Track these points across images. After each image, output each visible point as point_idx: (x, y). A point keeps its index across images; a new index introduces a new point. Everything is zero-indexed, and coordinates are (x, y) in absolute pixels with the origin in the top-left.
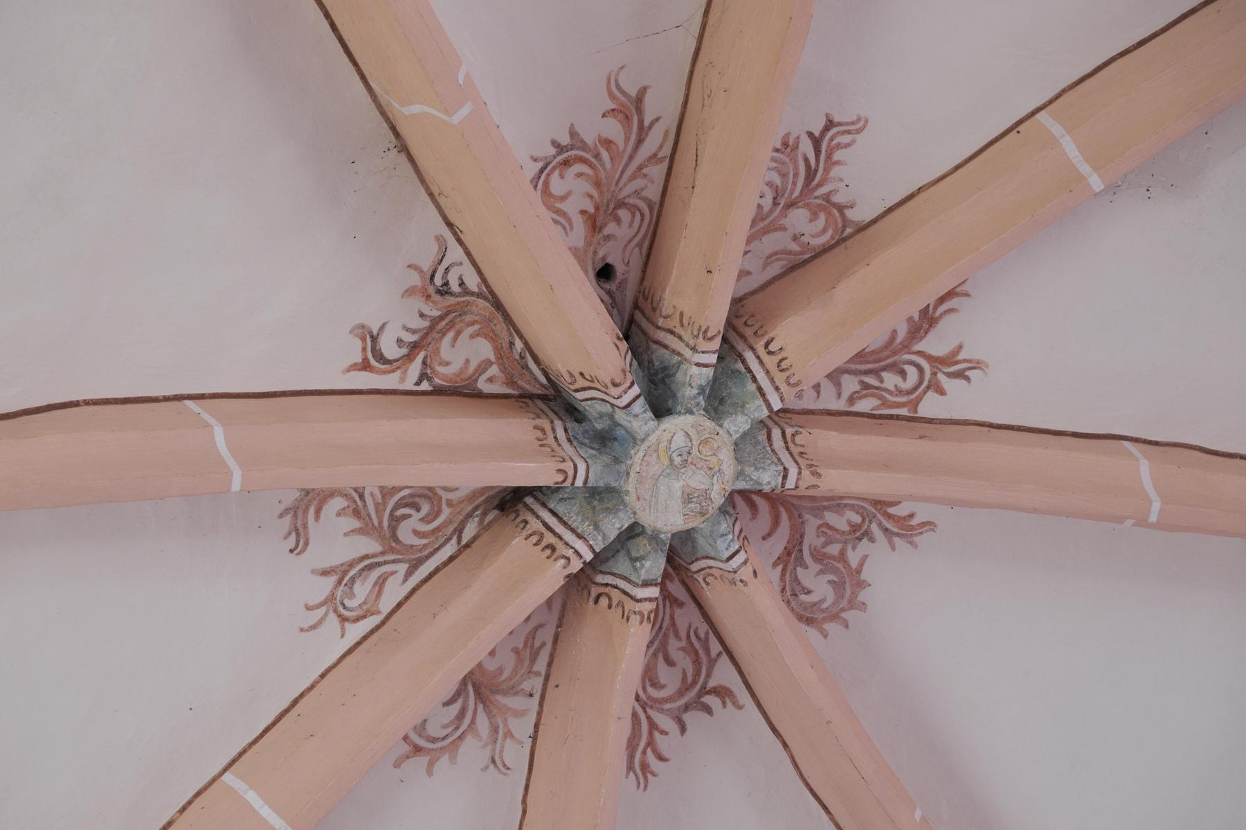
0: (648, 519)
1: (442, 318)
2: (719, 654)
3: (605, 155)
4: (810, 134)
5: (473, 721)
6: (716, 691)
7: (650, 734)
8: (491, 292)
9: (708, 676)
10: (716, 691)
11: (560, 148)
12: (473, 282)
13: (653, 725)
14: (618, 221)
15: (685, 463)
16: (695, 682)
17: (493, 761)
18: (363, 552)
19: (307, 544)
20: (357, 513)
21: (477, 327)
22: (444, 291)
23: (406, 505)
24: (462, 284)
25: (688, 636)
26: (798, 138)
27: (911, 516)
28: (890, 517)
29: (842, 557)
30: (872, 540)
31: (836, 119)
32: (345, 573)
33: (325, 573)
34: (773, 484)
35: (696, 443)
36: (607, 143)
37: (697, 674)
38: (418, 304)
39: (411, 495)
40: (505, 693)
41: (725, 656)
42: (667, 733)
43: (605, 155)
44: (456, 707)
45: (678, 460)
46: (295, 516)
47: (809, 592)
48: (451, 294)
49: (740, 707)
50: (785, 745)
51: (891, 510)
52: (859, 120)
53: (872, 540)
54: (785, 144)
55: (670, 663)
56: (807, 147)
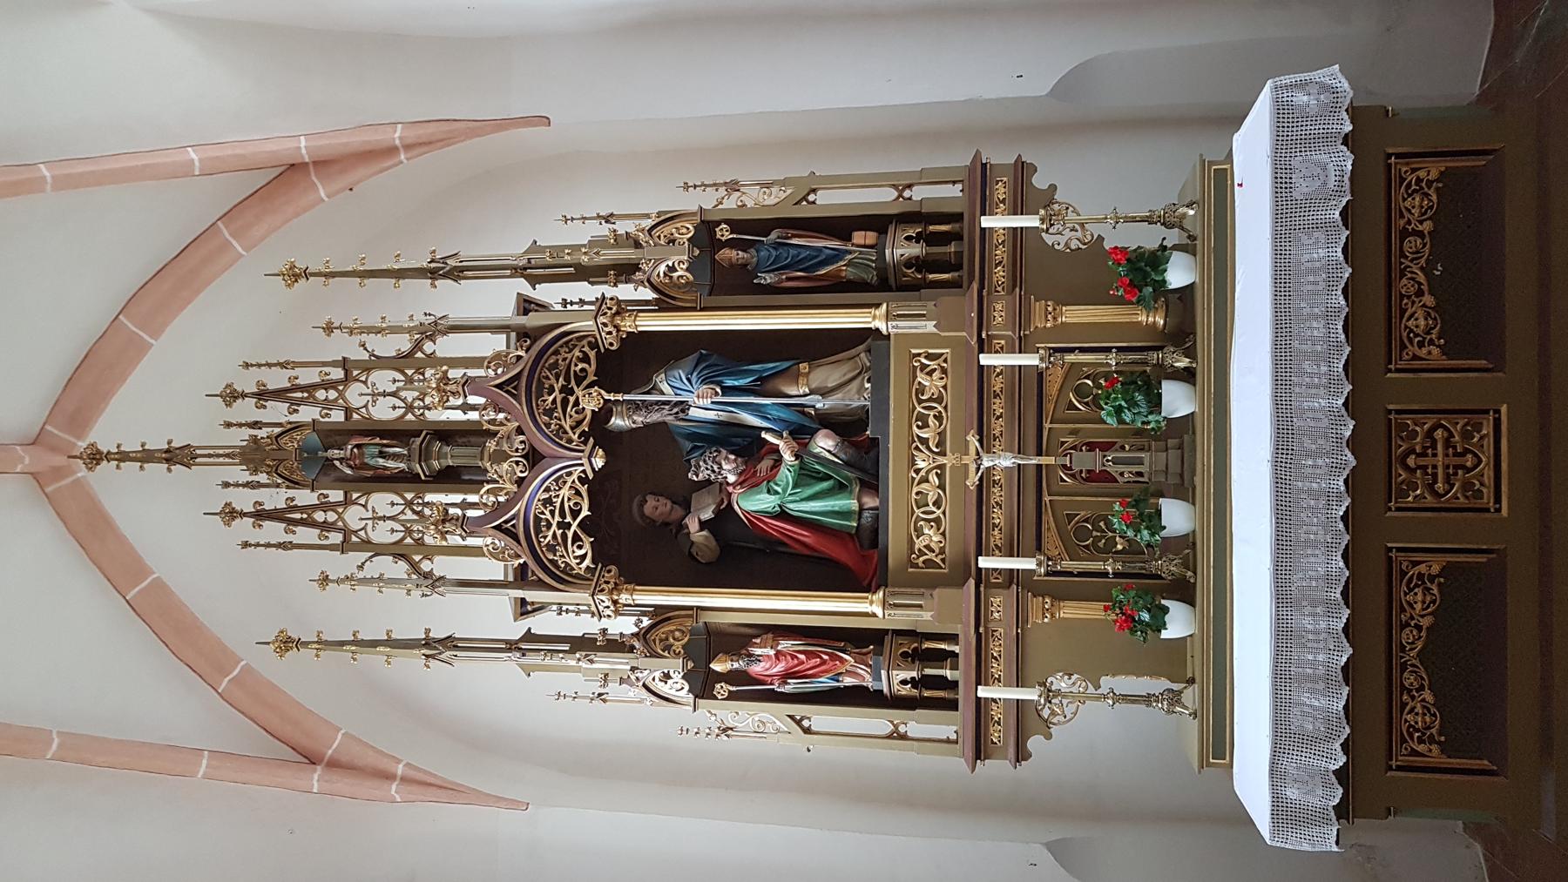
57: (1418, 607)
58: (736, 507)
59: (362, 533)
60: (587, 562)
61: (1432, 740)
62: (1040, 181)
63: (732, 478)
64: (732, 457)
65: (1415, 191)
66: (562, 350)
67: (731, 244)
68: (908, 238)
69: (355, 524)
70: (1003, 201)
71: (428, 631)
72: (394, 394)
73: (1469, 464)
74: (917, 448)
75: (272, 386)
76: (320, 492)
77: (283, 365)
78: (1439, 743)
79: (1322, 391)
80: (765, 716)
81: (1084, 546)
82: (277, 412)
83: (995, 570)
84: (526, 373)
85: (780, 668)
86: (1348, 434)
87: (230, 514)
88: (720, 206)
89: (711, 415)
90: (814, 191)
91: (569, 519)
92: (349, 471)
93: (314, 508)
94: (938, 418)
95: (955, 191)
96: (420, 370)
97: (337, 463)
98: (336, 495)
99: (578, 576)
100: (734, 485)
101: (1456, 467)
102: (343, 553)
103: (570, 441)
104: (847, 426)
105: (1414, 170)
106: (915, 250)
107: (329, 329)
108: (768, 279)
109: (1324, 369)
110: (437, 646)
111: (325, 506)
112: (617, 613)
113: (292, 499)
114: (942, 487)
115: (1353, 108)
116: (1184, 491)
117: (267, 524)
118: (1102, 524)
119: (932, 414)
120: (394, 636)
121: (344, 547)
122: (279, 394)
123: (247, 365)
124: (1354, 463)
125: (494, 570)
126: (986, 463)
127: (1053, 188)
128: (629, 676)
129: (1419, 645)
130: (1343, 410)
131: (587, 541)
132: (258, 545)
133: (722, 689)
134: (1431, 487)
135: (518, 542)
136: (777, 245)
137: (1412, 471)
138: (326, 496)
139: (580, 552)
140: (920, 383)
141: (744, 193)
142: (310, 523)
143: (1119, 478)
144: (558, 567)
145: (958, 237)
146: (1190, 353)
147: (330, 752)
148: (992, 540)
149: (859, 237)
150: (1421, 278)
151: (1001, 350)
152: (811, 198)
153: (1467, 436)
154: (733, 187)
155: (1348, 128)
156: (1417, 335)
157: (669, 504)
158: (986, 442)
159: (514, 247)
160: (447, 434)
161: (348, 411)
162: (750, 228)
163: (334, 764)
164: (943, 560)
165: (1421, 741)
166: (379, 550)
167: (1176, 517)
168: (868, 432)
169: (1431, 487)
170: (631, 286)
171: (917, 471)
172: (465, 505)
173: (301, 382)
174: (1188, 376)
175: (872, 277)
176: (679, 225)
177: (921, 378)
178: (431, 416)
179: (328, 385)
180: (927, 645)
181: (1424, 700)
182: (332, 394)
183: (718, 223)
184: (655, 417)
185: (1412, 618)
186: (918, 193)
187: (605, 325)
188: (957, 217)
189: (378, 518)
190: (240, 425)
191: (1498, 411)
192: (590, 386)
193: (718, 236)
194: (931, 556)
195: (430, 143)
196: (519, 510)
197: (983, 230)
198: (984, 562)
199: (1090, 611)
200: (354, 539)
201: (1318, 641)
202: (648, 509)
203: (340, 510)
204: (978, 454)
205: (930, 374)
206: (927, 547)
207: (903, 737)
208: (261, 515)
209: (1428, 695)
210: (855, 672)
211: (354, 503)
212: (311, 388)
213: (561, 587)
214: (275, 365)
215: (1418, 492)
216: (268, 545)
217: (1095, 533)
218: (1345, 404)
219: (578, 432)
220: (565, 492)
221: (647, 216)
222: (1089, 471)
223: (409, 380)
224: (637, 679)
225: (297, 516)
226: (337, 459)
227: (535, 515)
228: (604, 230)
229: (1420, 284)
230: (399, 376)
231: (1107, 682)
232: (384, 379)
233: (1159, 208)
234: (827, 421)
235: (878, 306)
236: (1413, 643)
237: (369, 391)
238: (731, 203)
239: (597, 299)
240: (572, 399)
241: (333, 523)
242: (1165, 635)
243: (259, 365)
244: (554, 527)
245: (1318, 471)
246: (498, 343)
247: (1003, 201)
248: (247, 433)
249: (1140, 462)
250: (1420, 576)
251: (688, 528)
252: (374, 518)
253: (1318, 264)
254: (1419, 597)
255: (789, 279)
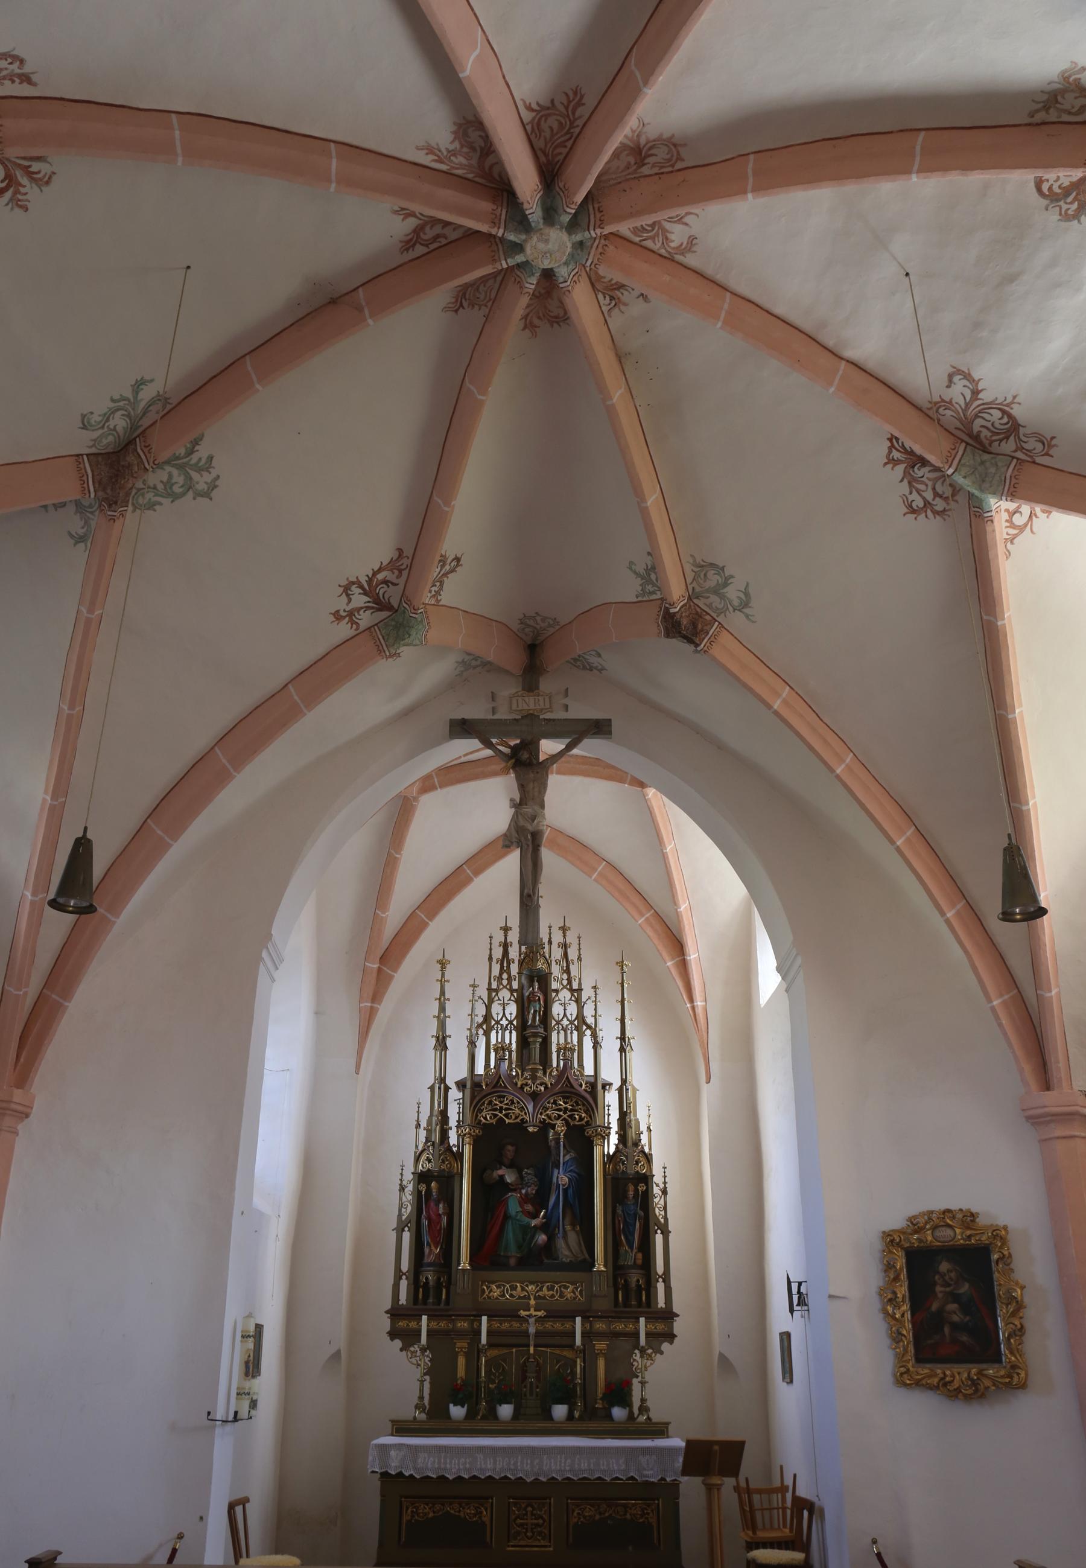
0: (564, 236)
1: (615, 289)
2: (527, 124)
3: (541, 315)
4: (464, 308)
5: (647, 143)
6: (532, 110)
7: (568, 105)
8: (594, 290)
9: (534, 119)
10: (532, 110)
11: (557, 323)
12: (600, 296)
13: (567, 108)
14: (539, 292)
15: (545, 253)
16: (542, 116)
17: (643, 124)
18: (669, 223)
19: (690, 237)
20: (667, 239)
21: (602, 280)
22: (612, 298)
23: (646, 230)
24: (605, 297)
25: (540, 136)
26: (468, 307)
27: (427, 154)
28: (438, 156)
29: (462, 146)
30: (447, 149)
31: (454, 313)
32: (679, 220)
33: (686, 224)
34: (509, 234)
35: (540, 259)
36: (539, 318)
37: (540, 119)
38: (623, 298)
39: (642, 232)
40: (629, 146)
41: (525, 121)
42: (561, 103)
43: (541, 315)
44: (651, 152)
45: (548, 255)
46: (690, 249)
47: (480, 136)
48: (609, 295)
49: (522, 100)
50: (504, 77)
51: (436, 158)
52: (445, 311)
53: (447, 149)
54: (473, 306)
55: (551, 128)
56: (465, 304)
57: (468, 1511)
58: (510, 1194)
59: (496, 998)
60: (483, 1121)
61: (413, 1516)
62: (665, 1346)
63: (523, 1191)
64: (534, 1192)
65: (643, 1511)
66: (585, 1108)
67: (636, 1190)
68: (638, 1281)
69: (501, 994)
70: (656, 1328)
71: (450, 1037)
72: (565, 1015)
73: (528, 1534)
74: (537, 1286)
75: (569, 950)
76: (517, 976)
77: (580, 959)
78: (412, 1519)
79: (558, 1468)
80: (409, 1209)
81: (491, 1370)
82: (557, 953)
83: (481, 1324)
84: (574, 1091)
85: (434, 1217)
86: (540, 1478)
87: (506, 929)
88: (654, 1185)
89: (555, 1180)
90: (662, 1233)
91: (504, 1112)
92: (527, 994)
93: (509, 974)
94: (552, 1296)
95: (661, 1303)
96: (577, 1028)
97: (531, 989)
98: (515, 985)
99: (477, 1116)
100: (521, 1193)
101: (527, 1529)
102: (487, 989)
103: (541, 1114)
104: (549, 1248)
105: (652, 1511)
106: (633, 1285)
107: (595, 988)
108: (619, 1211)
109: (567, 1468)
110: (441, 1043)
111: (509, 979)
112: (459, 1136)
113: (513, 962)
114: (520, 1298)
115: (678, 1484)
116: (516, 1416)
117: (501, 949)
118: (501, 1377)
119: (555, 1293)
120: (447, 1019)
121: (490, 990)
122: (566, 955)
123: (579, 938)
124: (528, 1481)
125: (480, 1070)
126: (531, 1320)
127: (662, 1353)
128: (430, 1141)
129: (452, 1512)
130: (550, 1477)
131: (494, 1121)
132: (491, 944)
133: (423, 1188)
134: (518, 1517)
135: (494, 1087)
136: (635, 1214)
137: (525, 1509)
138: (515, 980)
139: (488, 1118)
140: (569, 1287)
141: (661, 1198)
142: (502, 971)
143: (523, 1385)
144: (481, 1106)
145: (640, 1304)
146: (581, 1418)
147: (385, 969)
148: (494, 1323)
149: (640, 1255)
150: (607, 1515)
151: (583, 1325)
152: (659, 1231)
153: (540, 1533)
154: (664, 1192)
155: (668, 1479)
156: (582, 1512)
157: (510, 1158)
158: (539, 1320)
159: (636, 1078)
160: (546, 1042)
161: (557, 991)
162: (646, 1198)
163: (379, 970)
164: (485, 1298)
165: (412, 1512)
166: (488, 1008)
167: (506, 1411)
168: (546, 1261)
169: (518, 1517)
170: (617, 1142)
171: (527, 1286)
172: (510, 1052)
173: (571, 967)
174: (570, 1417)
175: (621, 1262)
176: (645, 1165)
177: (571, 1287)
178: (554, 1035)
179: (569, 980)
180: (444, 1291)
181: (429, 1513)
182: (565, 982)
183: (647, 1184)
184: (554, 1152)
185: (464, 1508)
186: (661, 1286)
187: (596, 1131)
188: (649, 1304)
189: (504, 1005)
190: (550, 934)
191: (550, 1547)
192: (567, 1123)
193: (640, 1185)
194: (487, 1293)
195: (696, 1020)
196: (507, 1088)
197: (638, 1319)
198: (484, 1319)
199: (461, 1372)
200: (494, 994)
201: (455, 1464)
202: (510, 1148)
203: (508, 987)
204: (535, 1316)
205: (573, 1292)
206: (491, 1291)
207: (401, 1278)
208: (506, 946)
209: (431, 1515)
210: (432, 1253)
211: (512, 994)
212: (567, 971)
213: (472, 1108)
214: (579, 953)
215: (517, 1512)
216: (491, 949)
217: (497, 1374)
218: (553, 1478)
219: (545, 1118)
220: (517, 1111)
221: (650, 1149)
222: (526, 1371)
223: (571, 1022)
224: (429, 1147)
225: (505, 965)
226: (533, 989)
227: (505, 1096)
228: (643, 1128)
229: (604, 1514)
230: (574, 1017)
231: (427, 1378)
232: (572, 1009)
233: (649, 1404)
234: (551, 1238)
235: (605, 1266)
236: (453, 1508)
237: (567, 1002)
238: (656, 1191)
239: (610, 1123)
240: (561, 1113)
241: (502, 984)
242: (451, 1406)
243: (579, 944)
244: (501, 1105)
245: (525, 1465)
246: (589, 1070)
247: (656, 1328)
248: (546, 940)
249: (531, 1394)
250: (481, 1513)
251: (500, 1168)
252: (504, 1004)
253: (611, 1466)
254: (473, 1512)
255: (619, 1221)
